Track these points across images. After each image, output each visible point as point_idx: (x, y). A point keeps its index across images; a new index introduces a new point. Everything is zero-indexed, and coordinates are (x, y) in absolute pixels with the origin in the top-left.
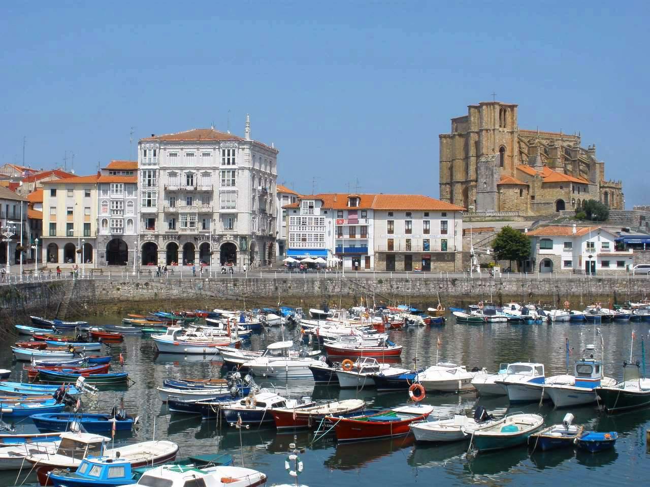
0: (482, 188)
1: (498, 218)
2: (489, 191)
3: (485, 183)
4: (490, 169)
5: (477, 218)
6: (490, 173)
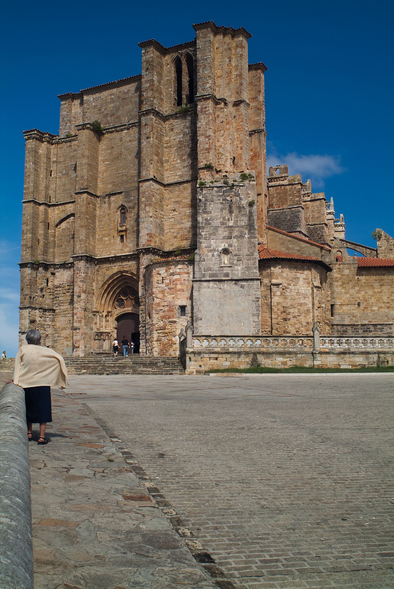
0: (216, 268)
1: (360, 360)
2: (240, 276)
3: (226, 251)
4: (240, 208)
5: (280, 359)
6: (244, 221)
